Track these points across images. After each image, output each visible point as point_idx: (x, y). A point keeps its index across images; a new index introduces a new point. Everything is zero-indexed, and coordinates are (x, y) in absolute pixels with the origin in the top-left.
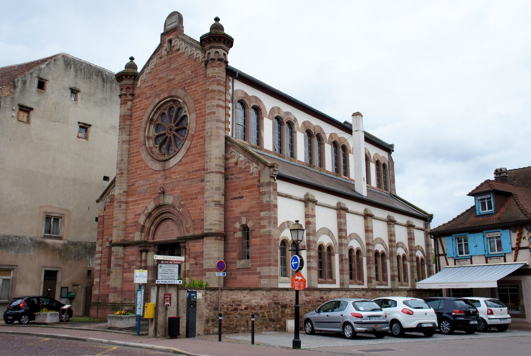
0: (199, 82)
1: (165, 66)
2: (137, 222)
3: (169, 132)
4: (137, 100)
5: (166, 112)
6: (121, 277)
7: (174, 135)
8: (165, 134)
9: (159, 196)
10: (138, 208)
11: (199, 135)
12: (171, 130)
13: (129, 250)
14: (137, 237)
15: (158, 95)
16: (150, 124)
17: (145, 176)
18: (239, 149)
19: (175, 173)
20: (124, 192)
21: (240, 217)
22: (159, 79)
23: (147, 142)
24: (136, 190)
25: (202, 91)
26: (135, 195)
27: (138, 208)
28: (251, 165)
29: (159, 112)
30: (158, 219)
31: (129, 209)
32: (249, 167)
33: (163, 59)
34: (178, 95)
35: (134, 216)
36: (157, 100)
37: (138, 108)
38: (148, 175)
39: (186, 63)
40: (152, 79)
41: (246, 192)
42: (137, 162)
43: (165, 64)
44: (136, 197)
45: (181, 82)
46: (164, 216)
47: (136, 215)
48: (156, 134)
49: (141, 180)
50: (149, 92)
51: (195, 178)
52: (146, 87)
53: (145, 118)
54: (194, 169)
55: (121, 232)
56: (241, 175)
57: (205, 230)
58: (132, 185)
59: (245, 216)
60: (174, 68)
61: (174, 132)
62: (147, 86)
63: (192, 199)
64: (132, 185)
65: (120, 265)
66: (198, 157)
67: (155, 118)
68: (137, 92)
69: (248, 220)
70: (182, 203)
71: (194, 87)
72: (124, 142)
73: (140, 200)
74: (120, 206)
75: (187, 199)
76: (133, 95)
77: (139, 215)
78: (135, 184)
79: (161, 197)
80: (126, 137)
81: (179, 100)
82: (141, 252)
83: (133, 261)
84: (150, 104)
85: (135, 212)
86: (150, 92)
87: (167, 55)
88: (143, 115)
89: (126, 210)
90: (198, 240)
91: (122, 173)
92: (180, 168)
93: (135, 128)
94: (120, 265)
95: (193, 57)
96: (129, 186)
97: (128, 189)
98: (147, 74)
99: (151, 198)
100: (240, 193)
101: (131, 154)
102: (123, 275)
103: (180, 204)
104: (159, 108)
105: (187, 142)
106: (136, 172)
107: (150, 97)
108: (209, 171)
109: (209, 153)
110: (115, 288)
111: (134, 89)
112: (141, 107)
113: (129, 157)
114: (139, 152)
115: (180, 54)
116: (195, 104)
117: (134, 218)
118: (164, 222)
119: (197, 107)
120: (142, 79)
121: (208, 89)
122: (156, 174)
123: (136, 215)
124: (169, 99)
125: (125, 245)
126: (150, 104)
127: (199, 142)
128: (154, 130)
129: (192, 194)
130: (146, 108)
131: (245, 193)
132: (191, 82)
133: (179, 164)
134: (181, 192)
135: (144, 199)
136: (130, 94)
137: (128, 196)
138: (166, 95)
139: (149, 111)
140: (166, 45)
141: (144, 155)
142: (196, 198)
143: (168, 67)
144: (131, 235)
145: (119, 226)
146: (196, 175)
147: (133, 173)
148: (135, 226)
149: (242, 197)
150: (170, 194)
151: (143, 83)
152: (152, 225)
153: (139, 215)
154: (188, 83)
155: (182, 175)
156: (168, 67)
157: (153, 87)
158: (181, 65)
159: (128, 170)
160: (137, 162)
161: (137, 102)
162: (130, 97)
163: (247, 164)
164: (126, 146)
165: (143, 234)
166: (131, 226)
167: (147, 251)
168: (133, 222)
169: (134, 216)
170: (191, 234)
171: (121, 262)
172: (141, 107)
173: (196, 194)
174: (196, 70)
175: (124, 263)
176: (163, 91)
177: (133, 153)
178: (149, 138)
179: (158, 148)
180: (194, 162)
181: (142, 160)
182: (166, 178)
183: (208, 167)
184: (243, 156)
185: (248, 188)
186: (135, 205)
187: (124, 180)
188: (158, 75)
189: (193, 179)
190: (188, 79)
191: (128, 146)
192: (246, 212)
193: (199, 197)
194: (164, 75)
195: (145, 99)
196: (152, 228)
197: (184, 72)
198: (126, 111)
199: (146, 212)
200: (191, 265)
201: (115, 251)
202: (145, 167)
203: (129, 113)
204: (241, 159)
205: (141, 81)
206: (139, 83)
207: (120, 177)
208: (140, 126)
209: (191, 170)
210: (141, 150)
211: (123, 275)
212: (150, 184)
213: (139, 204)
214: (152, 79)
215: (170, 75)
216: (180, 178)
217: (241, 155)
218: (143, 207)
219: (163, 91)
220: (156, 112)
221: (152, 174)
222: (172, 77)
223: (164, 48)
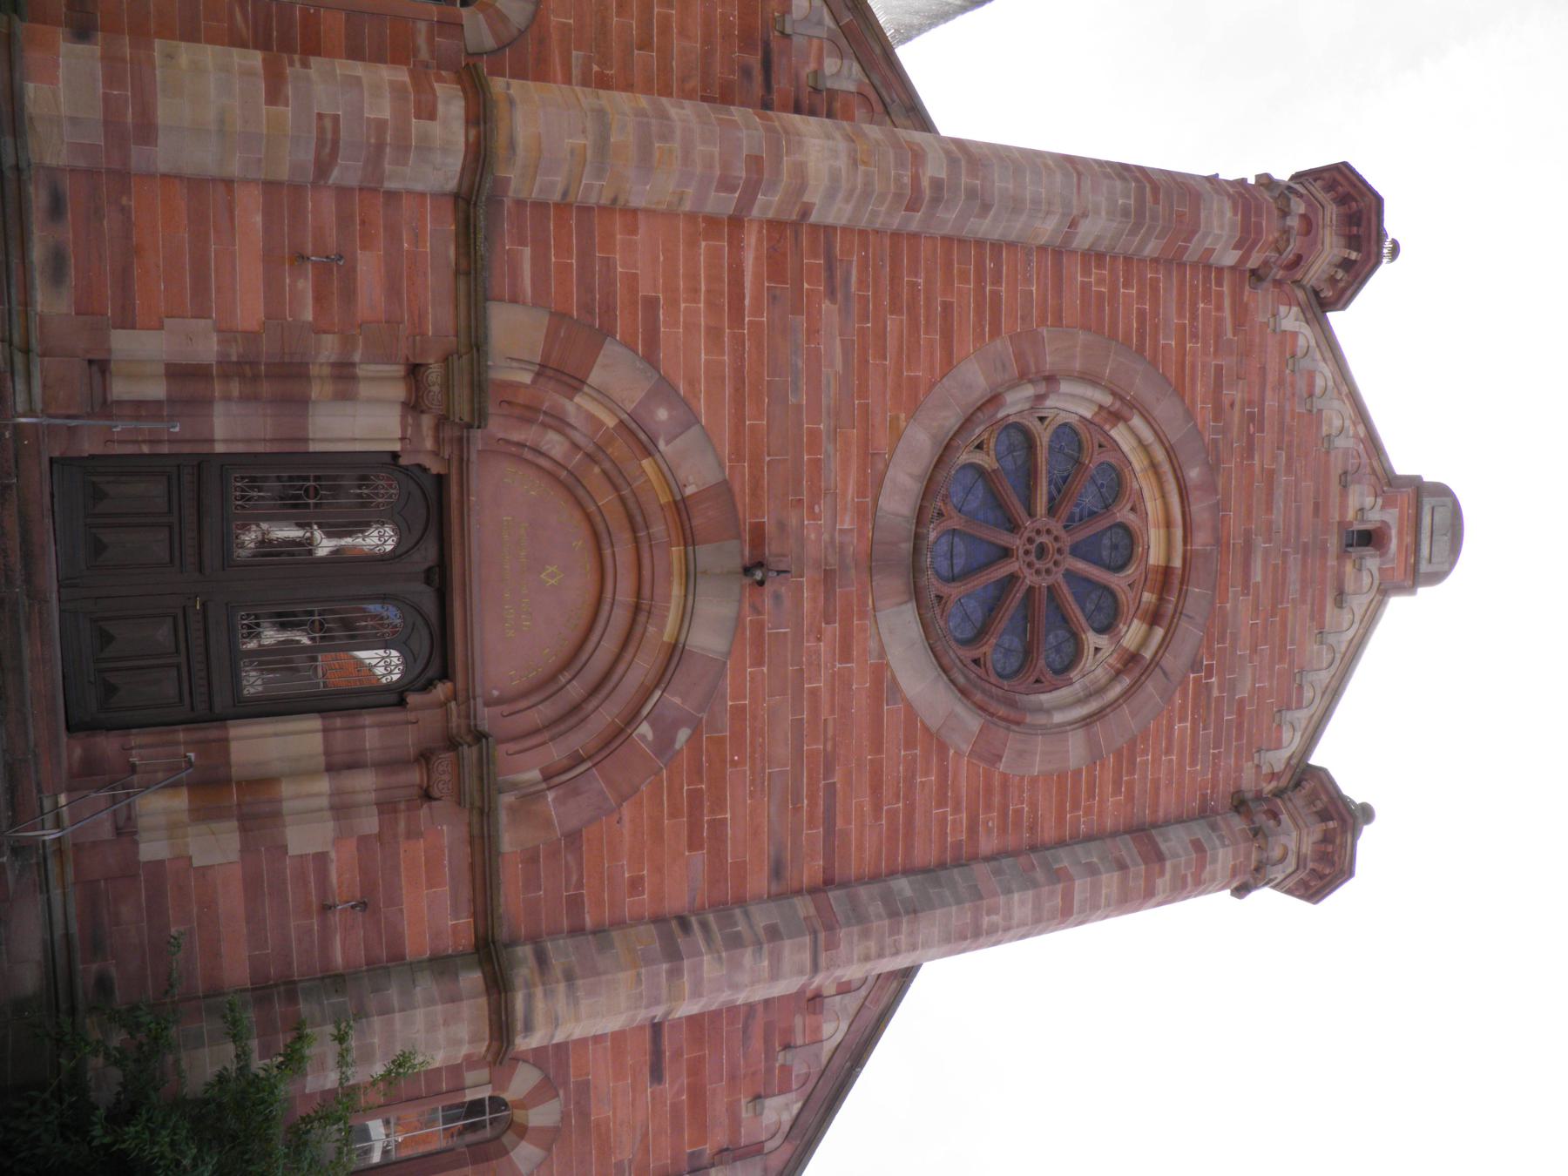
0: (1193, 764)
1: (1308, 510)
2: (607, 332)
3: (1039, 540)
4: (1227, 303)
5: (1123, 514)
6: (234, 169)
7: (1013, 578)
8: (1031, 514)
9: (739, 536)
10: (691, 328)
11: (989, 808)
12: (1042, 551)
13: (436, 240)
14: (516, 335)
15: (1213, 468)
16: (1101, 407)
17: (863, 392)
18: (873, 1011)
19: (846, 655)
20: (805, 212)
21: (565, 1084)
22: (1270, 476)
23: (1029, 391)
24: (797, 310)
25: (1156, 783)
26: (773, 299)
27: (691, 328)
28: (792, 1096)
29: (1138, 462)
30: (606, 498)
31: (692, 244)
32: (783, 1091)
33: (1335, 488)
34: (1184, 624)
35: (644, 290)
36: (1194, 474)
37: (1194, 317)
38: (865, 408)
39: (1281, 660)
40: (1282, 423)
41: (679, 1093)
42: (947, 307)
43: (1316, 505)
44: (757, 310)
45: (1222, 639)
46: (623, 553)
47: (651, 304)
48: (1044, 436)
49: (845, 353)
50: (1238, 396)
51: (797, 810)
52: (1263, 369)
53: (1141, 386)
54: (840, 794)
55: (560, 180)
56: (757, 1044)
57: (529, 998)
58: (830, 267)
59: (565, 1116)
60: (1284, 579)
61: (1016, 542)
62: (1263, 391)
63: (695, 796)
64: (830, 267)
65: (323, 168)
66: (893, 814)
67: (1119, 433)
68: (1260, 299)
69: (549, 1138)
70: (683, 735)
71: (1183, 731)
72: (1073, 224)
73: (739, 341)
74: (726, 185)
75: (696, 772)
76: (1256, 275)
77: (651, 359)
78: (831, 293)
79: (733, 554)
80: (1088, 233)
81: (1159, 632)
82: (414, 371)
83: (349, 294)
84: (1189, 414)
85: (674, 303)
86: (1237, 407)
87: (1342, 524)
88: (1154, 363)
89: (691, 217)
90: (465, 893)
91: (912, 207)
92: (861, 685)
93: (1114, 290)
94: (323, 168)
95: (1289, 708)
96: (829, 230)
97: (815, 227)
98: (1311, 376)
99: (737, 455)
100: (677, 1054)
101: (997, 257)
102: (246, 182)
103: (676, 725)
104: (1154, 466)
105: (974, 722)
106: (895, 308)
107: (1218, 412)
108: (823, 958)
109: (903, 938)
110: (147, 131)
111: (1278, 283)
112: (1194, 336)
113: (980, 243)
114: (996, 332)
115: (1322, 610)
116: (1119, 754)
117: (632, 280)
118: (580, 542)
119: (1102, 765)
120: (1301, 341)
121: (1162, 873)
122: (861, 493)
123: (651, 304)
124: (1177, 563)
125: (473, 204)
126: (1189, 414)
127: (957, 810)
128: (1073, 420)
129: (719, 804)
130: (1179, 391)
131: (674, 1086)
132: (1209, 696)
133: (883, 684)
134: (739, 712)
135: (738, 390)
136: (1266, 263)
137: (775, 227)
138: (1201, 539)
139: (1166, 409)
140: (1375, 517)
141: (974, 376)
142: (694, 844)
143: (1298, 528)
144: (527, 251)
145: (599, 172)
146: (812, 823)
147: (895, 280)
148: (587, 308)
149: (657, 1074)
150: (739, 619)
151: (1282, 353)
152: (576, 446)
153: (651, 359)
154: (1208, 687)
155: (825, 713)
156: (1298, 528)
157: (1254, 419)
158: (1284, 625)
159: (915, 236)
160: (947, 307)
161: (1219, 308)
162: (1253, 263)
163: (799, 1069)
164: (1048, 229)
165: (526, 378)
166: (585, 255)
167: (413, 407)
168: (608, 264)
169: (644, 290)
170: (510, 841)
171: (347, 172)
172: (1194, 336)
173: (718, 826)
174: (1239, 738)
175: (343, 192)
176: (1219, 509)
177: (997, 280)
178: (1040, 398)
179: (978, 458)
180: (876, 789)
181: (949, 364)
182: (829, 576)
183: (843, 948)
184: (839, 1037)
185: (697, 1095)
186: (712, 306)
187: (874, 214)
188: (1289, 470)
189: (797, 798)
190: (1221, 690)
191: (1042, 241)
192: (584, 1114)
193: (699, 859)
194: (1277, 516)
195: (1219, 368)
196: (554, 444)
197: (1254, 650)
198: (1208, 243)
199: (662, 414)
200: (321, 858)
201: (435, 128)
202: (914, 381)
203: (1193, 253)
204: (827, 1029)
205: (1295, 335)
206: (1291, 319)
207: (898, 196)
208: (1113, 336)
209: (837, 778)
210: (1003, 346)
211: (246, 182)
212: (814, 435)
213: (714, 334)
214: (1282, 423)
215: (1267, 552)
216: (814, 693)
217: (844, 1026)
218: (692, 382)
219: (1219, 509)
220: (1145, 448)
221: (868, 455)
222: (1257, 576)
223: (1369, 501)
